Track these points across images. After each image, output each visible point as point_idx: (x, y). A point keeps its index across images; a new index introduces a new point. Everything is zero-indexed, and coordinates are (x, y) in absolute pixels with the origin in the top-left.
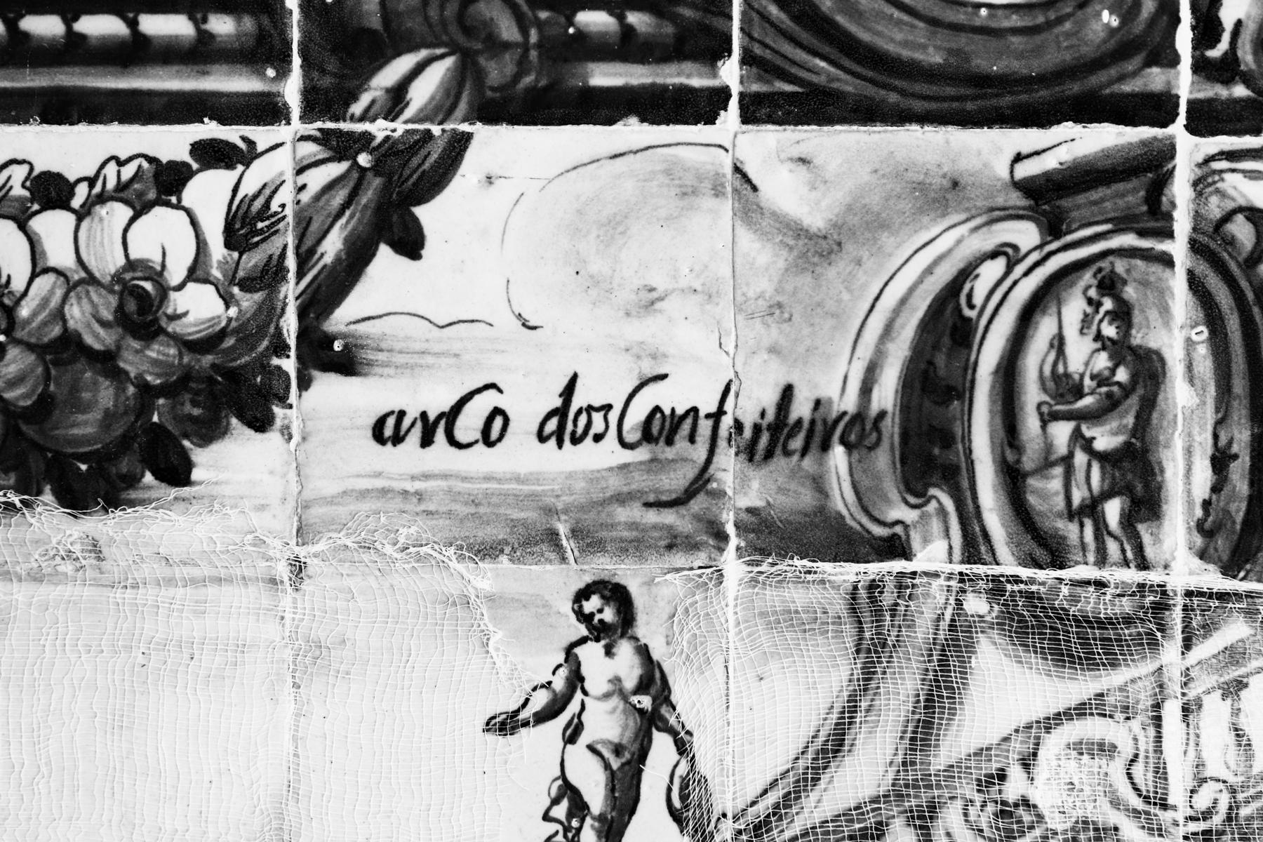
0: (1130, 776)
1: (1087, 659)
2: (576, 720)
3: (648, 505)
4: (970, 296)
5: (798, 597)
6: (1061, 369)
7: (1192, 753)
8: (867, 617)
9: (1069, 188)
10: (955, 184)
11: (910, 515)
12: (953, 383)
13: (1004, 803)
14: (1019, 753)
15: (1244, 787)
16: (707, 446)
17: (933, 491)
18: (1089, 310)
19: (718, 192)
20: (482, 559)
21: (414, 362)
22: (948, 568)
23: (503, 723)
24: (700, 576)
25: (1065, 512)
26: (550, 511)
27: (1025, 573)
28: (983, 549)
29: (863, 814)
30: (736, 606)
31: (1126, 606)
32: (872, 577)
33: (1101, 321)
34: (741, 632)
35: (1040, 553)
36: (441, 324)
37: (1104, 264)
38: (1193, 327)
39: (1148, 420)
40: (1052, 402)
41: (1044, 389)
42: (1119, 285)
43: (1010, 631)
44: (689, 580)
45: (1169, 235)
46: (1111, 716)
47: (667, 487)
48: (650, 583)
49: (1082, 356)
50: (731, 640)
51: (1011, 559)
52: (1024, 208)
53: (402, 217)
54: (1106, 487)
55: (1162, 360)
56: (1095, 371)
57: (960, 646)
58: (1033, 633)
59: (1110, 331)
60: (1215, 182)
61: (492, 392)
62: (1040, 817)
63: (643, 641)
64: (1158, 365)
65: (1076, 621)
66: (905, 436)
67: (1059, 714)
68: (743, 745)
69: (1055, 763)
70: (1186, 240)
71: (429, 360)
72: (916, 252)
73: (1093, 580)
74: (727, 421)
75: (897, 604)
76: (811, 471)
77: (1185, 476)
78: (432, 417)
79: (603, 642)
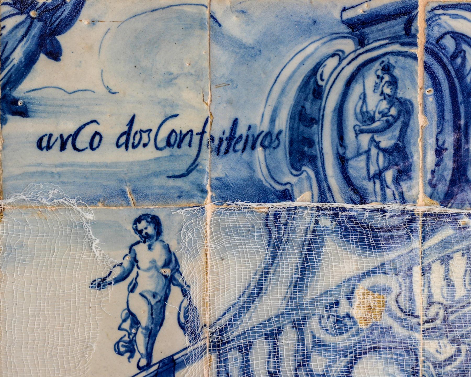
0: (397, 302)
1: (377, 247)
2: (134, 281)
3: (169, 177)
4: (321, 75)
5: (240, 220)
6: (364, 109)
7: (426, 291)
8: (273, 229)
9: (368, 23)
10: (315, 22)
11: (293, 180)
12: (314, 116)
13: (338, 316)
14: (345, 292)
15: (451, 306)
16: (197, 148)
17: (304, 168)
18: (378, 81)
19: (202, 27)
20: (89, 205)
21: (57, 110)
22: (312, 204)
23: (99, 284)
24: (194, 211)
25: (367, 177)
26: (121, 181)
27: (348, 206)
28: (328, 195)
29: (271, 323)
30: (211, 225)
31: (395, 221)
32: (275, 210)
33: (383, 86)
34: (213, 237)
35: (355, 197)
36: (70, 92)
37: (385, 59)
38: (426, 89)
39: (406, 133)
40: (361, 125)
41: (357, 119)
42: (392, 69)
43: (341, 234)
44: (188, 212)
45: (416, 45)
46: (388, 274)
47: (178, 168)
48: (170, 215)
49: (375, 103)
50: (208, 241)
51: (341, 199)
52: (347, 33)
53: (51, 41)
54: (386, 165)
55: (412, 104)
56: (381, 110)
57: (317, 242)
58: (352, 235)
59: (387, 91)
60: (436, 20)
61: (94, 124)
62: (355, 323)
63: (166, 242)
64: (410, 106)
65: (373, 229)
66: (291, 142)
67: (364, 273)
68: (214, 291)
69: (362, 297)
70: (423, 47)
71: (65, 109)
72: (296, 54)
73: (382, 209)
74: (207, 136)
75: (287, 223)
76: (247, 159)
77: (423, 157)
78: (65, 137)
79: (147, 243)
